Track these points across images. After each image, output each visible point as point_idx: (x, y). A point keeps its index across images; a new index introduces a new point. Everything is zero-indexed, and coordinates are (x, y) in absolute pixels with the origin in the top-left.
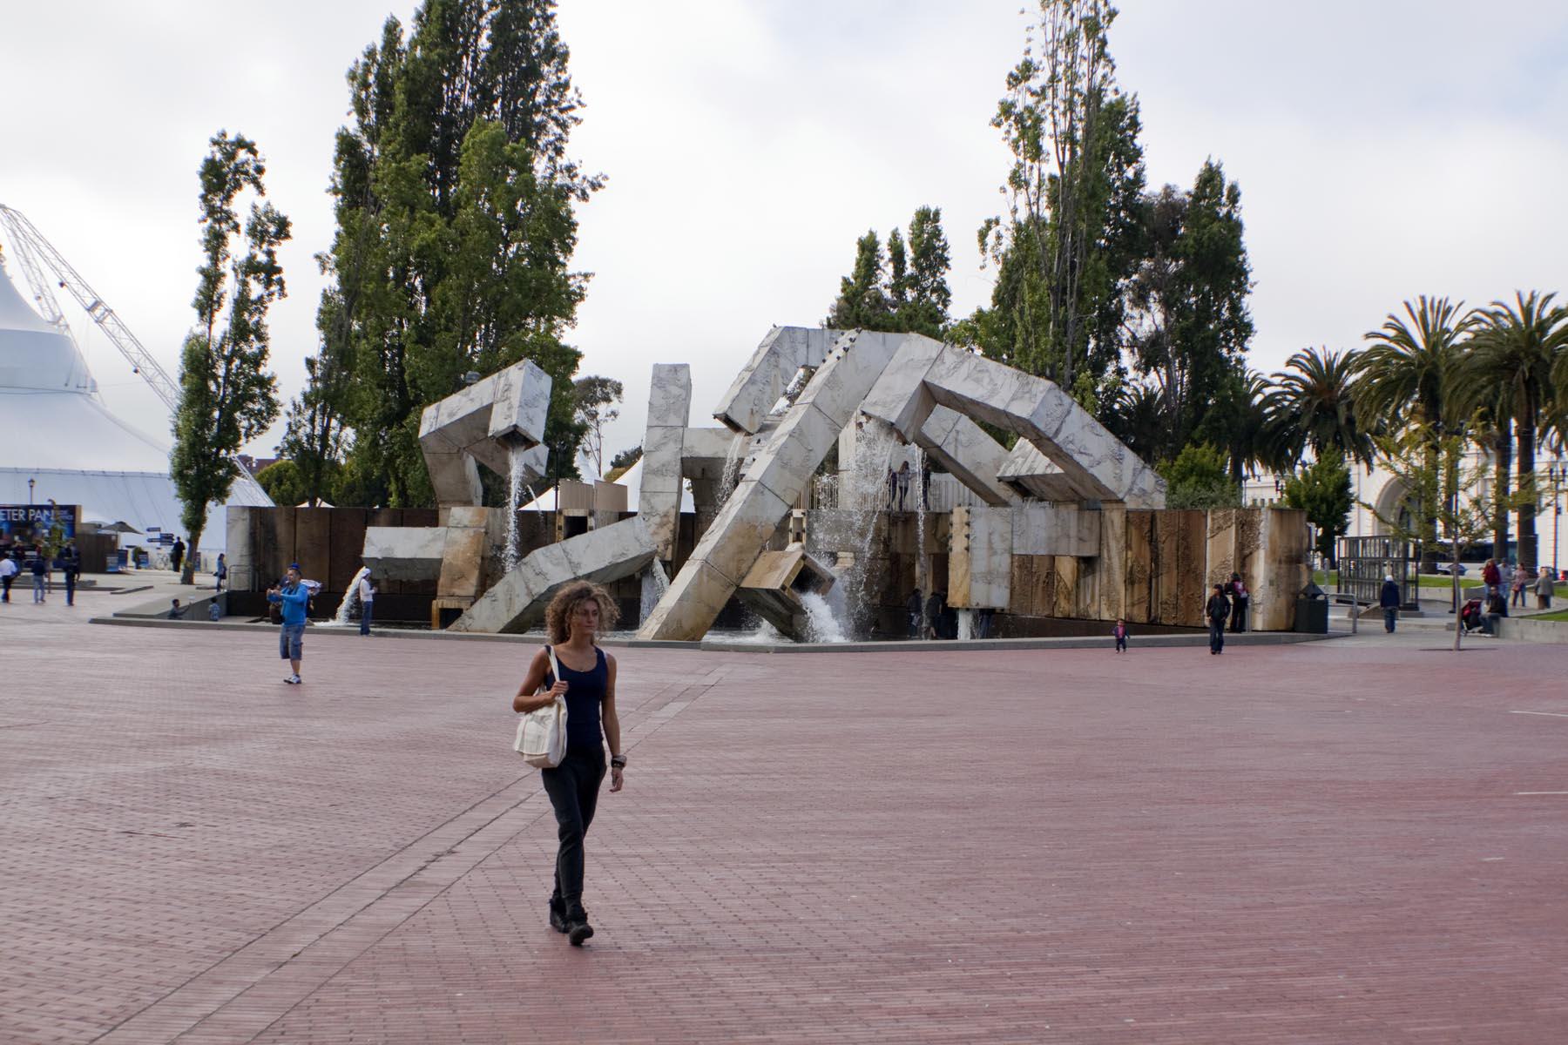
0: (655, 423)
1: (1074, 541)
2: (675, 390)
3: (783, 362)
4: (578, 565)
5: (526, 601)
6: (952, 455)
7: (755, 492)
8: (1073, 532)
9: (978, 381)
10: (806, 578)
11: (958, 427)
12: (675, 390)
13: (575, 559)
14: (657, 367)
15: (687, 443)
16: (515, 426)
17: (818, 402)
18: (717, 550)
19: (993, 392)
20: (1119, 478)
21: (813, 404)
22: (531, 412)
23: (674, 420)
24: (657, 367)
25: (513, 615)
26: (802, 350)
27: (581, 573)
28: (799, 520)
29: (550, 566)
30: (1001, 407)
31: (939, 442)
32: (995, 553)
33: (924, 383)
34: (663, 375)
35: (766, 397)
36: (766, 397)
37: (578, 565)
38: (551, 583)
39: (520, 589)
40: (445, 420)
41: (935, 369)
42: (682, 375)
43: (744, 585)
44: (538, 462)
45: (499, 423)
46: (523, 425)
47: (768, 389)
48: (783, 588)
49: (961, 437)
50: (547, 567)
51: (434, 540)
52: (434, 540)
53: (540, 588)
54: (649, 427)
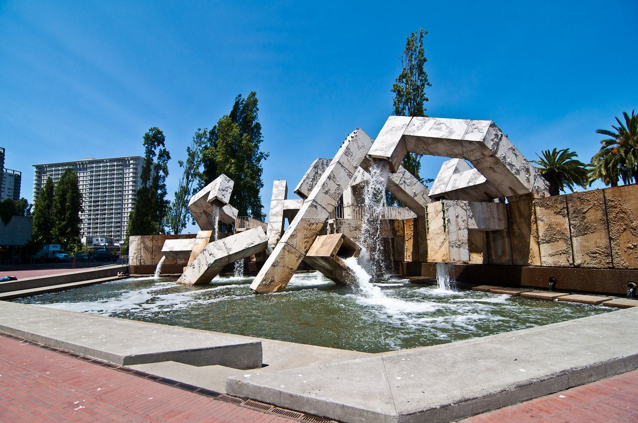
1: (496, 221)
5: (206, 268)
6: (403, 188)
8: (496, 215)
9: (438, 129)
10: (346, 249)
11: (405, 176)
13: (229, 247)
16: (216, 197)
17: (341, 161)
19: (451, 132)
20: (528, 180)
21: (338, 162)
22: (224, 193)
27: (231, 253)
28: (331, 225)
29: (216, 250)
30: (459, 138)
31: (397, 182)
32: (460, 229)
33: (404, 136)
40: (196, 200)
41: (410, 129)
43: (312, 253)
45: (210, 197)
46: (220, 197)
48: (332, 255)
49: (407, 181)
51: (190, 243)
52: (190, 243)
53: (211, 261)
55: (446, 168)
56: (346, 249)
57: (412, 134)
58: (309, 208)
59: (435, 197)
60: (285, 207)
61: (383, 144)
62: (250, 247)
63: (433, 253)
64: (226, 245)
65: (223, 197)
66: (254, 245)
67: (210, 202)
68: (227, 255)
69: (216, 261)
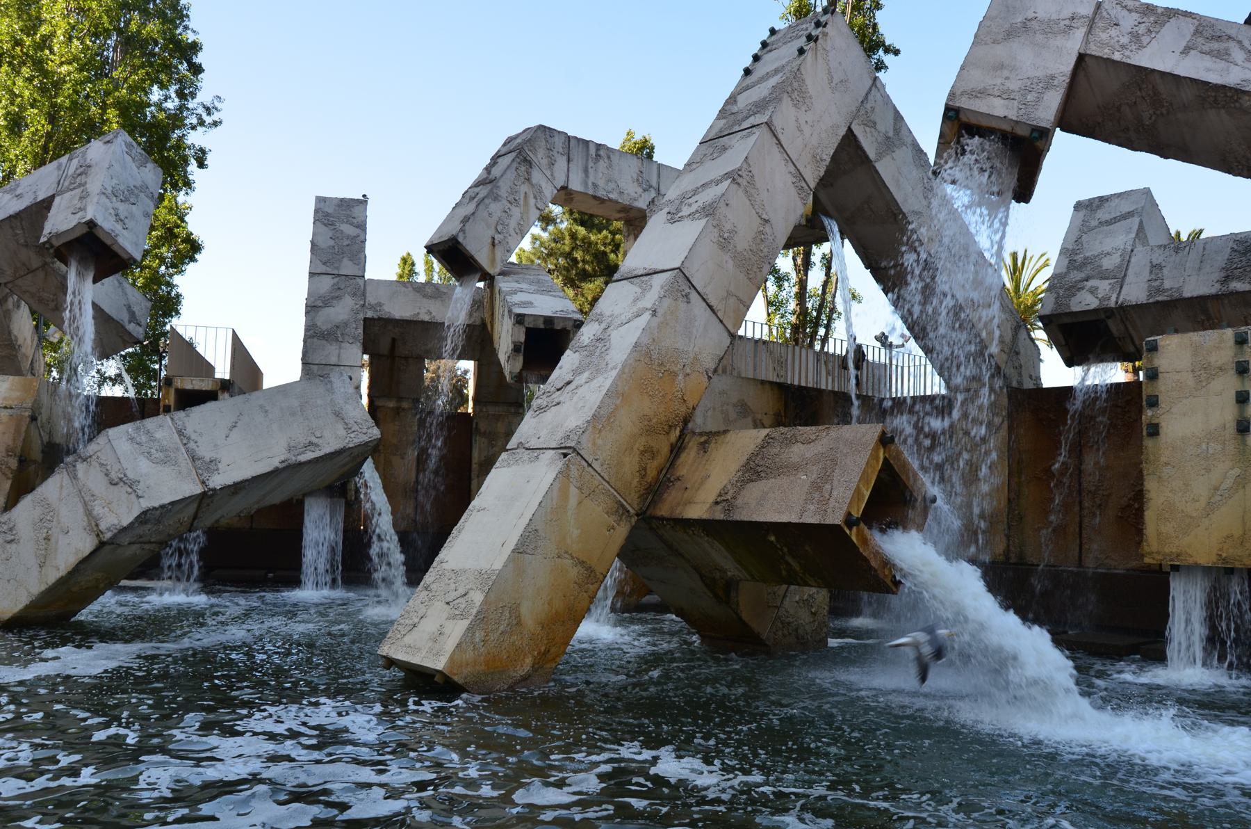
0: (322, 269)
2: (348, 229)
3: (536, 176)
4: (212, 465)
5: (86, 545)
7: (670, 291)
12: (348, 229)
13: (205, 452)
14: (320, 200)
15: (371, 299)
17: (778, 124)
18: (600, 421)
23: (347, 268)
24: (320, 200)
25: (53, 576)
26: (561, 162)
27: (217, 481)
29: (144, 465)
34: (330, 210)
35: (513, 223)
36: (513, 223)
37: (212, 465)
38: (146, 504)
39: (70, 516)
42: (356, 211)
44: (133, 318)
45: (60, 221)
46: (106, 223)
47: (516, 212)
48: (850, 521)
50: (141, 468)
54: (312, 274)
55: (1094, 223)
56: (891, 499)
57: (1117, 57)
58: (667, 302)
59: (1066, 320)
60: (372, 307)
61: (1006, 73)
62: (303, 458)
63: (1167, 528)
64: (192, 445)
65: (119, 227)
66: (318, 454)
67: (56, 243)
68: (198, 489)
69: (144, 517)
